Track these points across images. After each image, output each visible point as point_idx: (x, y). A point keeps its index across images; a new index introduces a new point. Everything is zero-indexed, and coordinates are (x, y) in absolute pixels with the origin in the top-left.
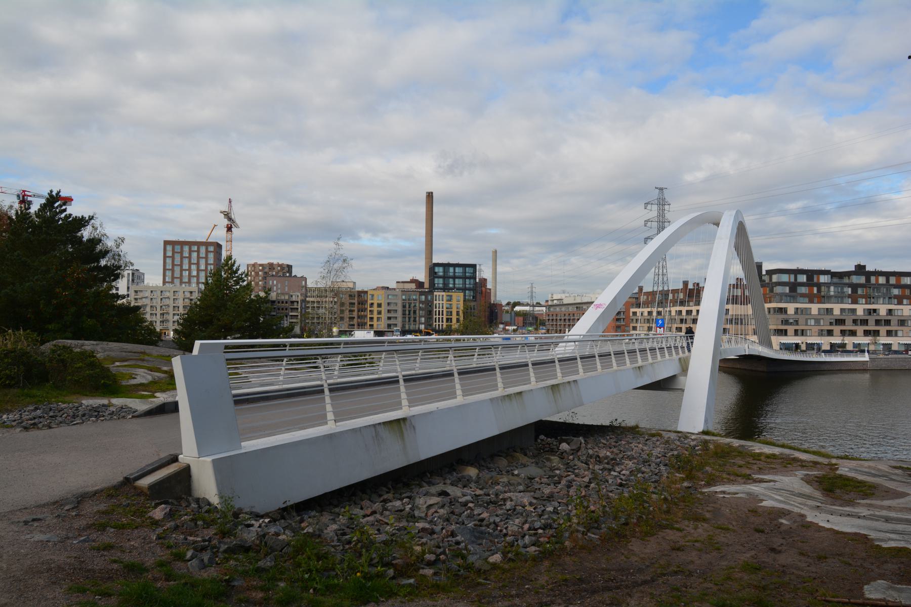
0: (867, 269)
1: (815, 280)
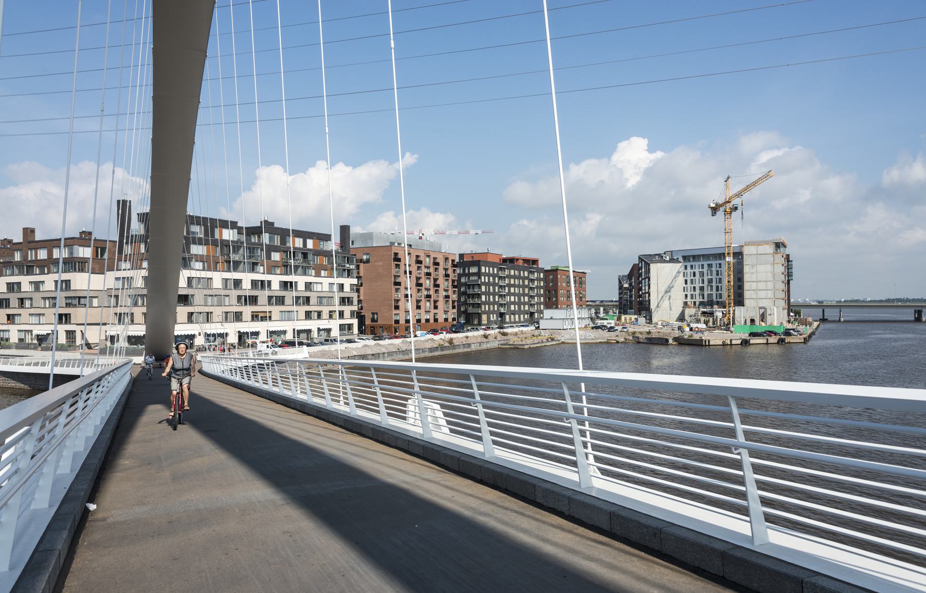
0: (275, 226)
1: (217, 236)
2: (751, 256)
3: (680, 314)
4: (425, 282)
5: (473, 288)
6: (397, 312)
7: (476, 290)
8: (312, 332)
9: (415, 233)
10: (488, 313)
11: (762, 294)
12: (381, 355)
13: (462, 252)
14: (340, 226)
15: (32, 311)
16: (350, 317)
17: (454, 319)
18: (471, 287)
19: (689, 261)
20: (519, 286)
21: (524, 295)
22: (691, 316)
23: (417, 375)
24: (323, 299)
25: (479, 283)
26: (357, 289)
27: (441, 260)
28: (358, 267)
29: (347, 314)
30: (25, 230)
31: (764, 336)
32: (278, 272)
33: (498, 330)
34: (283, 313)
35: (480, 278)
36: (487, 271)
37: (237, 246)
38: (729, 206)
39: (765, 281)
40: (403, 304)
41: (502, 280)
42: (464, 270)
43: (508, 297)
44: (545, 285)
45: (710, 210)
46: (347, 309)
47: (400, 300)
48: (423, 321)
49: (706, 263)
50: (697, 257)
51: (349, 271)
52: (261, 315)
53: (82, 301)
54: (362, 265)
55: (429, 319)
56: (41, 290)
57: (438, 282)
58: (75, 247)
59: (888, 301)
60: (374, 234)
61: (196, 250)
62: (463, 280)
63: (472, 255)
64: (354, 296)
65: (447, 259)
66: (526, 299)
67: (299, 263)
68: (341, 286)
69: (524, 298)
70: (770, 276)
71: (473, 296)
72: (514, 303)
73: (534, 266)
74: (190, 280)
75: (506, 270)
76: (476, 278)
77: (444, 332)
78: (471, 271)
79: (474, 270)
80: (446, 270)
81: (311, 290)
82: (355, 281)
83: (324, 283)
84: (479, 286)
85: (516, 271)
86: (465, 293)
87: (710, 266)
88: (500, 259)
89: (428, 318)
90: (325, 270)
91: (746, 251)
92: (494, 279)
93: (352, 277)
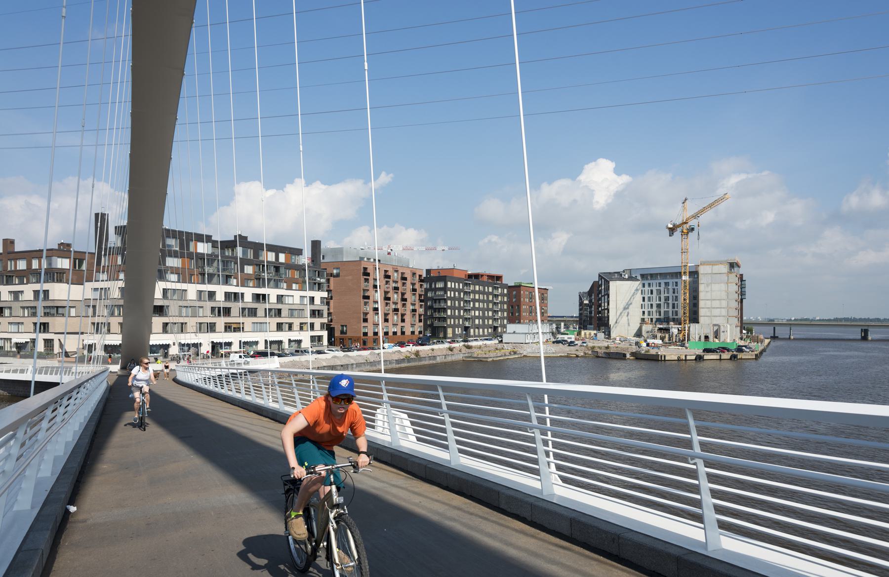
1: (192, 249)
2: (706, 275)
3: (638, 330)
4: (393, 296)
5: (439, 302)
6: (365, 324)
7: (442, 305)
8: (284, 344)
9: (384, 249)
10: (454, 327)
11: (716, 312)
12: (350, 366)
13: (429, 268)
14: (312, 241)
15: (12, 320)
16: (320, 329)
17: (420, 332)
18: (437, 301)
19: (647, 279)
20: (483, 301)
21: (488, 310)
22: (648, 332)
23: (386, 385)
24: (294, 311)
25: (445, 298)
26: (327, 302)
27: (408, 275)
28: (328, 281)
29: (317, 326)
30: (5, 241)
31: (717, 352)
32: (251, 284)
33: (463, 343)
34: (256, 325)
35: (446, 293)
36: (453, 286)
37: (211, 259)
38: (686, 227)
39: (719, 300)
40: (372, 317)
41: (467, 295)
42: (431, 286)
43: (473, 312)
44: (509, 299)
45: (668, 231)
46: (318, 322)
47: (368, 313)
48: (391, 334)
49: (663, 282)
50: (654, 276)
51: (319, 284)
52: (234, 326)
53: (60, 310)
54: (332, 279)
55: (396, 332)
56: (20, 300)
57: (406, 296)
58: (54, 258)
59: (836, 320)
60: (344, 250)
61: (172, 262)
62: (429, 295)
63: (439, 271)
64: (325, 308)
65: (414, 274)
66: (490, 314)
67: (271, 276)
68: (312, 299)
69: (488, 313)
70: (724, 295)
71: (439, 310)
72: (478, 317)
73: (498, 282)
74: (165, 291)
75: (472, 286)
76: (442, 293)
77: (411, 345)
78: (437, 286)
79: (440, 285)
80: (413, 284)
81: (282, 303)
82: (325, 294)
83: (295, 296)
84: (445, 301)
85: (481, 287)
86: (431, 307)
87: (667, 284)
88: (466, 275)
89: (396, 331)
90: (297, 283)
91: (702, 270)
92: (459, 294)
93: (322, 291)
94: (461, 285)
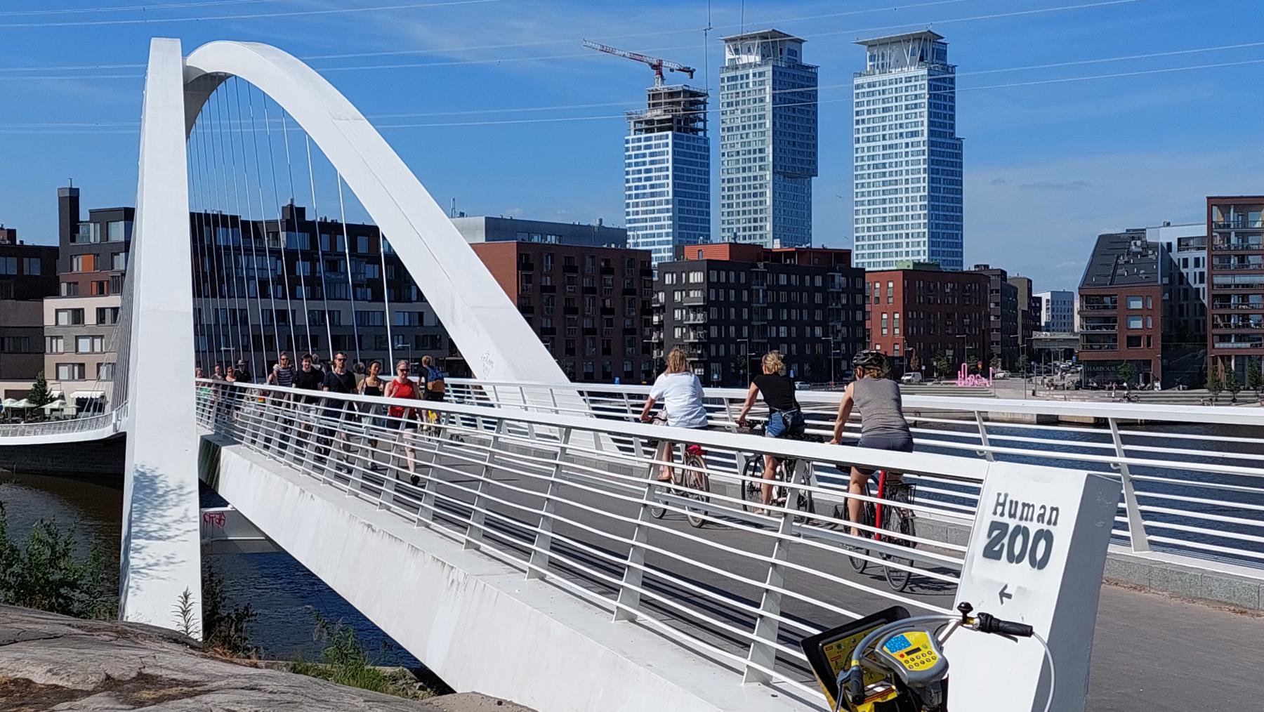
36: (723, 279)
42: (679, 278)
62: (677, 296)
78: (691, 281)
85: (793, 277)
92: (739, 295)
94: (743, 275)
